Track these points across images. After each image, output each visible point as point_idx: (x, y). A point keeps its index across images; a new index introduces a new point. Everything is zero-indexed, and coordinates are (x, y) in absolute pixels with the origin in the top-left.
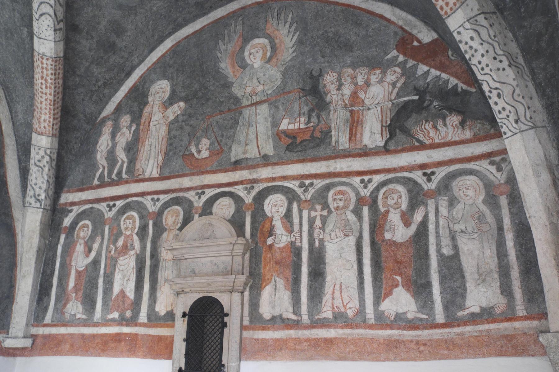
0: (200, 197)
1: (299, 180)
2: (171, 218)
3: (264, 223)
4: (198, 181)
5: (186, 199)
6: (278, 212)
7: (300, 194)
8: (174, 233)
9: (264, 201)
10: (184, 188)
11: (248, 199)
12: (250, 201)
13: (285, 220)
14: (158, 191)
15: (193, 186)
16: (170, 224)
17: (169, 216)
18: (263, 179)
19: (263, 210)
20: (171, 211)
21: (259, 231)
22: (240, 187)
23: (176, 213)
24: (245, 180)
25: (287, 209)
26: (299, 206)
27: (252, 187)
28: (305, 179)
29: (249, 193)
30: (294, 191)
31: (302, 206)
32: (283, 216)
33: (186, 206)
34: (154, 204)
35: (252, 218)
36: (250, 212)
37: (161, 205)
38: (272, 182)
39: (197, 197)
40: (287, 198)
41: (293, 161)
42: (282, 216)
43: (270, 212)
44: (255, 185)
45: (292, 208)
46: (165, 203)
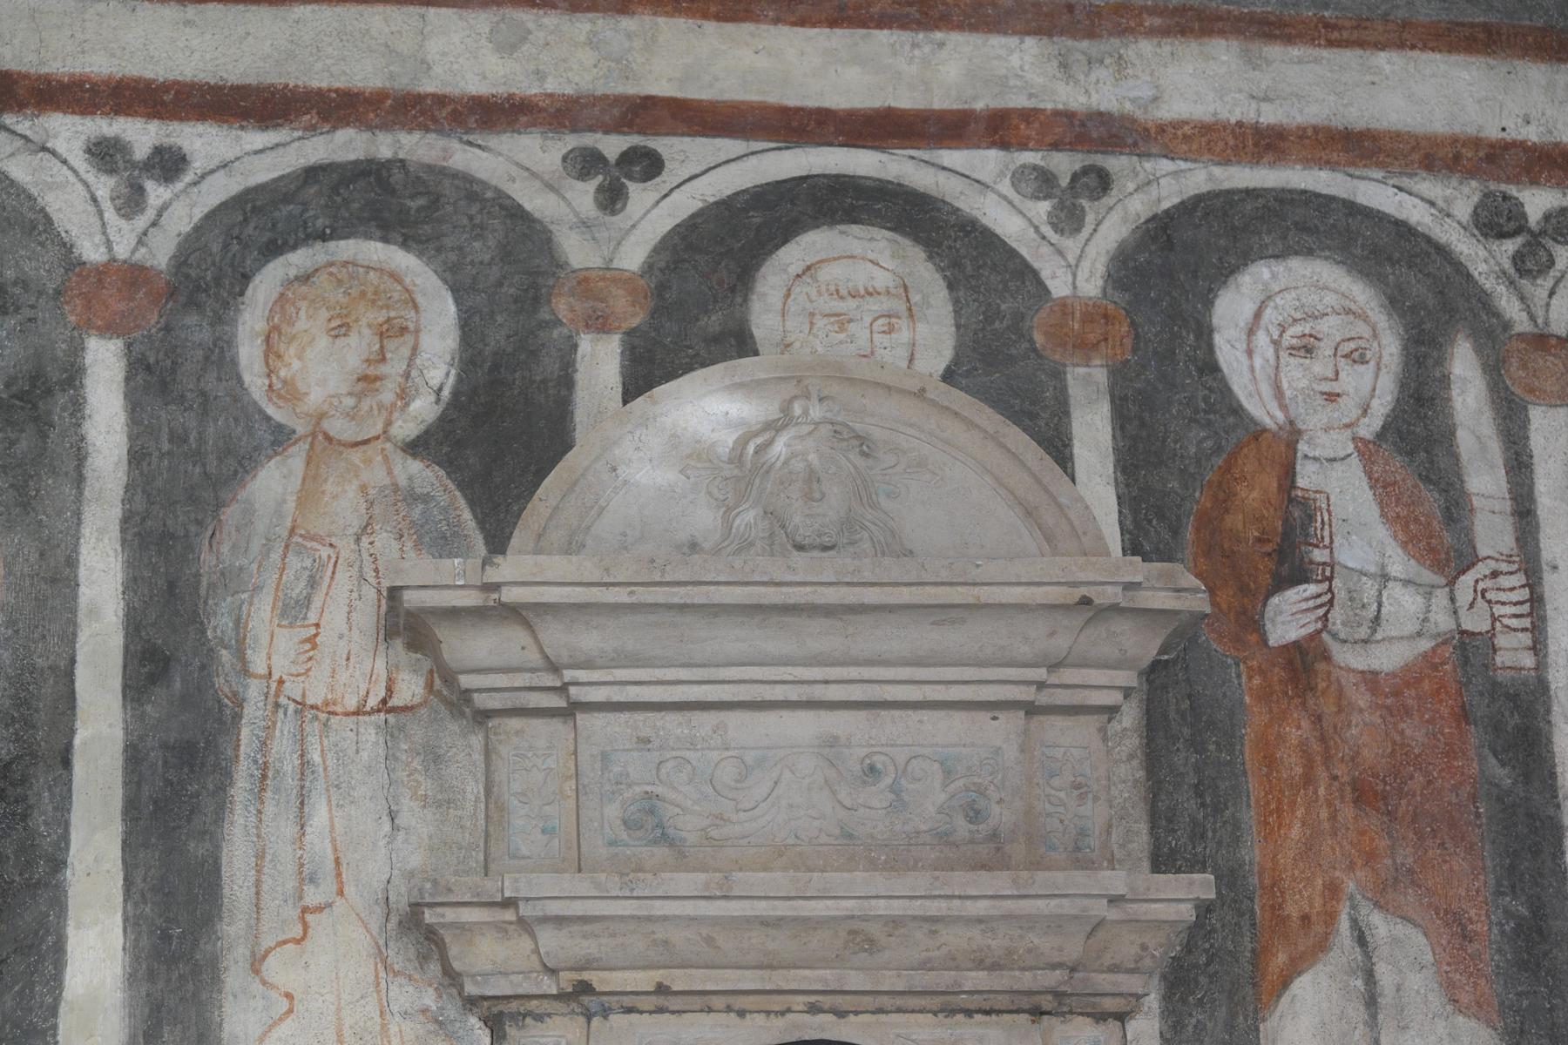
0: (612, 198)
1: (1471, 173)
2: (323, 342)
3: (1228, 468)
4: (587, 56)
5: (472, 197)
6: (1332, 397)
7: (1488, 284)
8: (377, 476)
9: (1209, 304)
10: (441, 100)
11: (1073, 269)
12: (1091, 285)
13: (1396, 466)
14: (166, 87)
15: (530, 89)
16: (315, 397)
17: (310, 323)
18: (1177, 125)
19: (1210, 367)
20: (322, 278)
21: (1189, 534)
22: (987, 161)
23: (375, 299)
24: (1028, 115)
25: (1403, 386)
26: (1494, 370)
27: (1092, 180)
28: (1514, 179)
29: (1069, 219)
30: (1443, 251)
31: (1514, 372)
32: (1381, 435)
33: (481, 251)
34: (132, 201)
35: (1120, 419)
36: (1100, 375)
37: (210, 217)
38: (1256, 159)
39: (584, 194)
40: (1395, 302)
41: (1405, 25)
42: (1370, 427)
43: (1266, 389)
44: (1115, 164)
45: (1445, 381)
46: (249, 203)
